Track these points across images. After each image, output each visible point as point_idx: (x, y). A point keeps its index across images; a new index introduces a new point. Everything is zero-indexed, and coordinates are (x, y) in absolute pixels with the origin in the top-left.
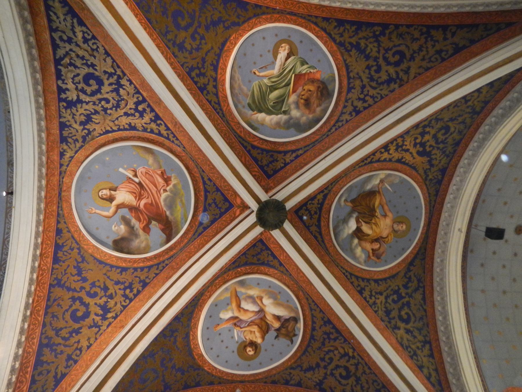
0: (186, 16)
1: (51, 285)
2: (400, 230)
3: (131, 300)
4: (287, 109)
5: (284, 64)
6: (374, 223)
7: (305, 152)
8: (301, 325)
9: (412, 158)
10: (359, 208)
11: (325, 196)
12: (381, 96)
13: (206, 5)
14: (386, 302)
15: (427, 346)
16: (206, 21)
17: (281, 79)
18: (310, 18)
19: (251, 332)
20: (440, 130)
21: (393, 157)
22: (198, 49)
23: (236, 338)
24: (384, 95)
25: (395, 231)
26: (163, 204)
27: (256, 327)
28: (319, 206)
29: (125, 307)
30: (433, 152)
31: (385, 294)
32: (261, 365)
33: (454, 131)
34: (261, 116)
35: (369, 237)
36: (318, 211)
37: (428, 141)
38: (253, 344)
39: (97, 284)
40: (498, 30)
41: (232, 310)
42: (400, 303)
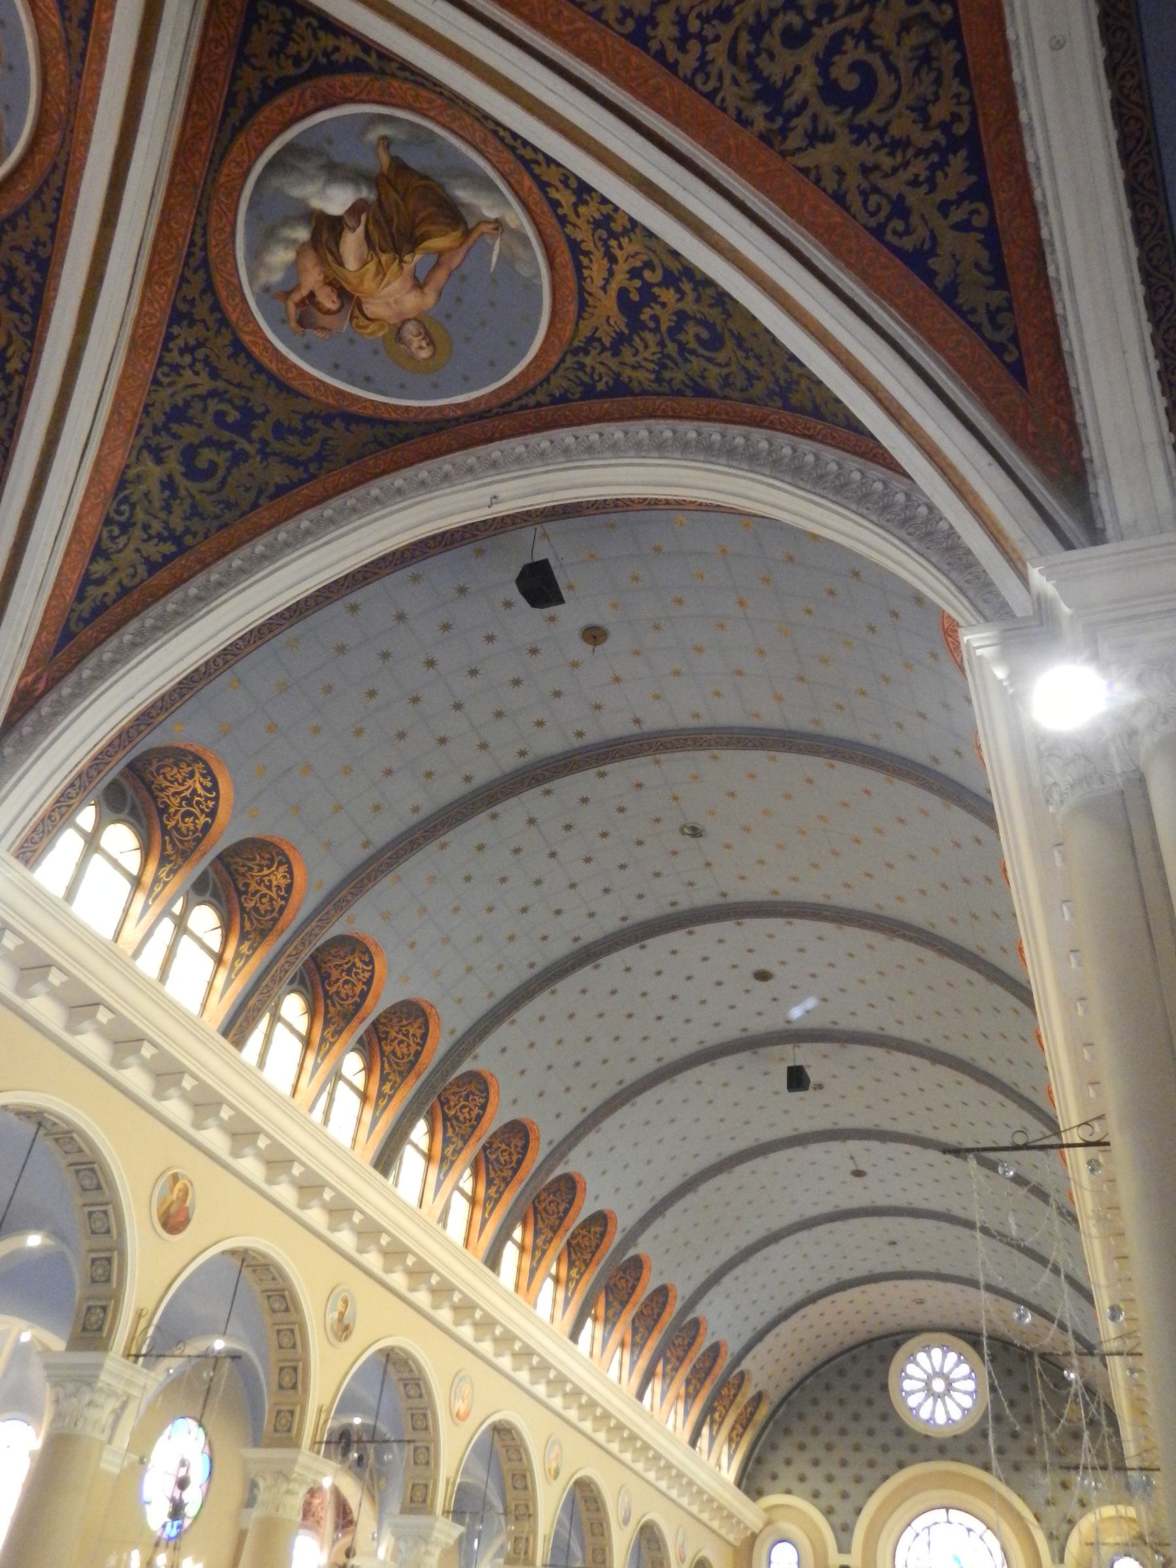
2: (409, 347)
9: (602, 283)
10: (393, 196)
11: (358, 66)
12: (716, 91)
14: (202, 398)
15: (169, 548)
20: (703, 323)
21: (575, 226)
24: (723, 100)
25: (398, 333)
28: (324, 61)
31: (221, 385)
35: (335, 266)
36: (306, 66)
37: (664, 305)
40: (998, 349)
42: (226, 436)
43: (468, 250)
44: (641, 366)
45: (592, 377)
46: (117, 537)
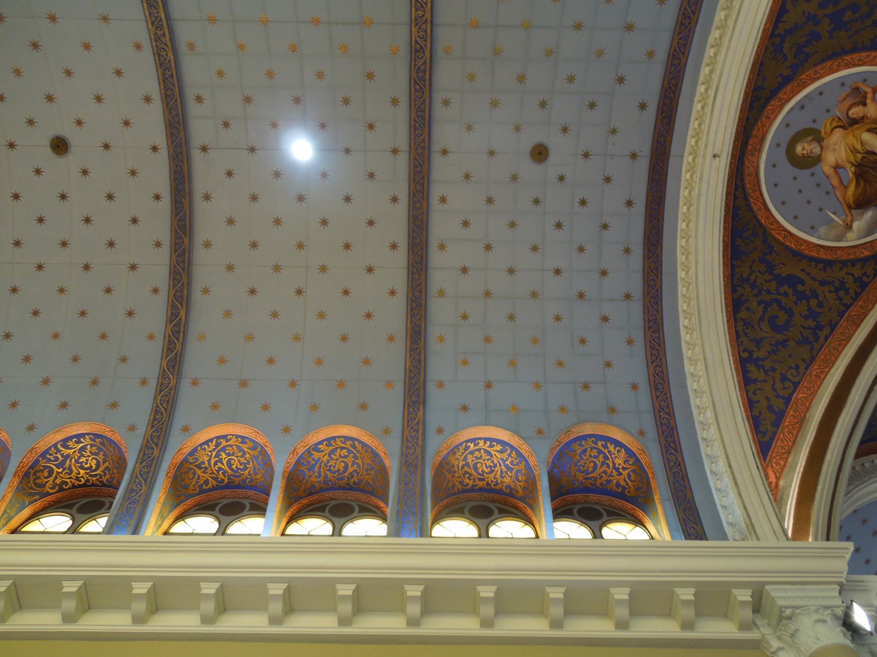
2: (808, 142)
6: (859, 153)
21: (841, 269)
30: (773, 285)
33: (759, 324)
35: (868, 127)
43: (841, 203)
44: (752, 272)
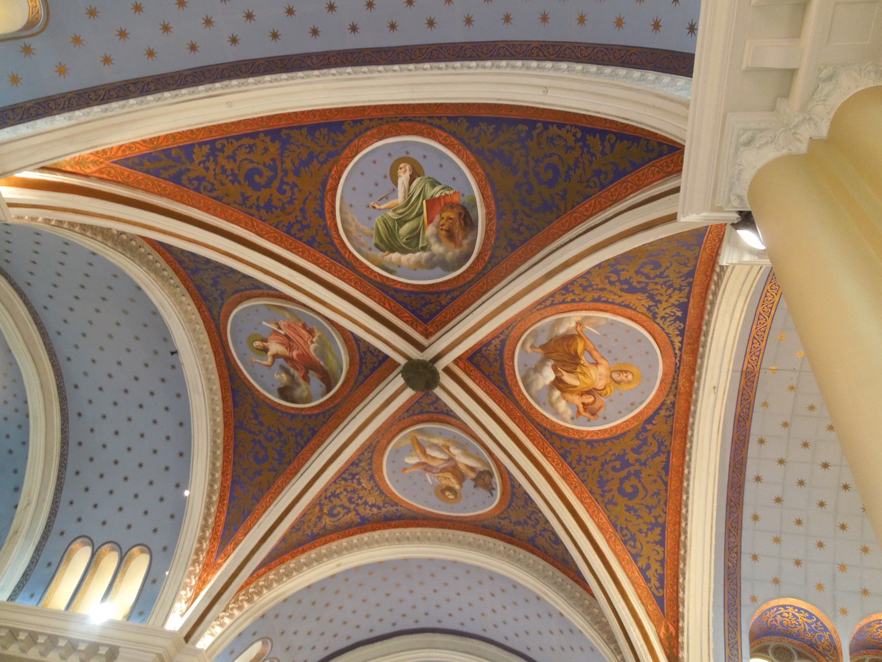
0: (264, 170)
1: (235, 427)
2: (624, 381)
3: (302, 448)
4: (425, 245)
5: (409, 190)
7: (461, 293)
8: (497, 480)
10: (554, 354)
13: (288, 146)
16: (293, 164)
17: (408, 210)
18: (431, 121)
19: (445, 478)
22: (291, 202)
23: (431, 482)
26: (314, 354)
27: (450, 474)
29: (297, 454)
32: (465, 509)
34: (395, 256)
36: (498, 358)
38: (450, 489)
39: (272, 429)
41: (418, 456)
42: (624, 473)
45: (673, 316)
46: (635, 545)
